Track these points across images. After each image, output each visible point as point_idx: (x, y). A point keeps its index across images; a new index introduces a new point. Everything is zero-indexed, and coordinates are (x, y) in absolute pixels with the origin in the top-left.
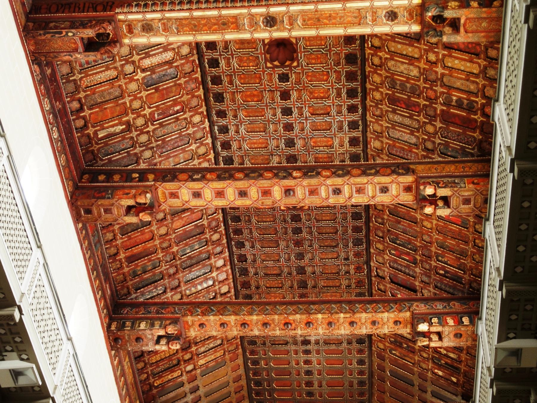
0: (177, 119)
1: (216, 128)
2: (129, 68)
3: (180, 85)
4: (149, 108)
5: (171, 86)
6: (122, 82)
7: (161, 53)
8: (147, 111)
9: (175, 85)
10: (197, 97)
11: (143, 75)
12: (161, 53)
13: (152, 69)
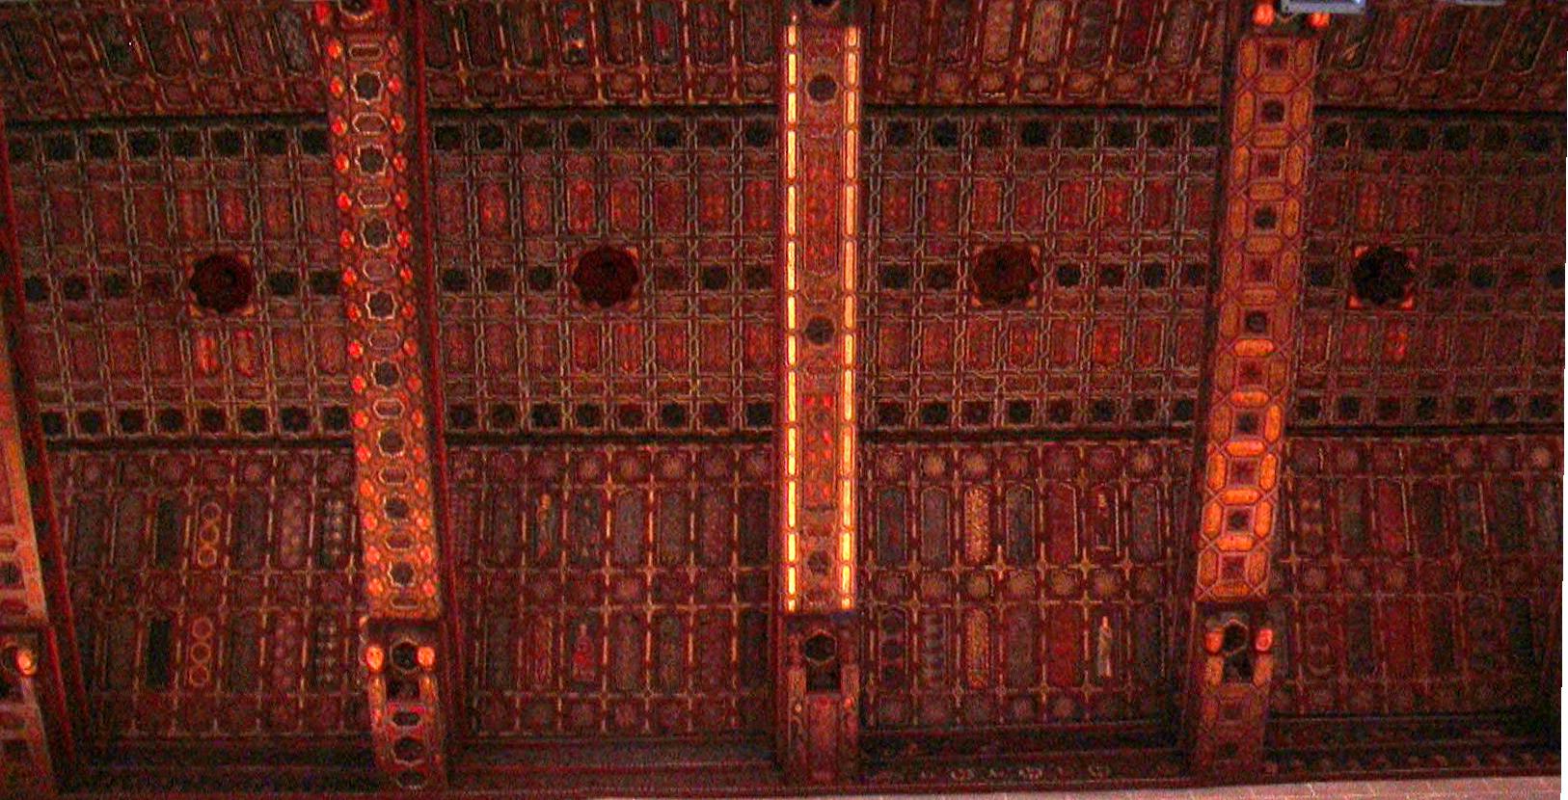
0: (1126, 506)
1: (1176, 424)
3: (1048, 488)
4: (1079, 560)
5: (1046, 509)
6: (1001, 605)
7: (962, 518)
8: (1085, 566)
9: (1045, 497)
10: (1088, 455)
11: (1000, 560)
12: (962, 518)
13: (994, 538)
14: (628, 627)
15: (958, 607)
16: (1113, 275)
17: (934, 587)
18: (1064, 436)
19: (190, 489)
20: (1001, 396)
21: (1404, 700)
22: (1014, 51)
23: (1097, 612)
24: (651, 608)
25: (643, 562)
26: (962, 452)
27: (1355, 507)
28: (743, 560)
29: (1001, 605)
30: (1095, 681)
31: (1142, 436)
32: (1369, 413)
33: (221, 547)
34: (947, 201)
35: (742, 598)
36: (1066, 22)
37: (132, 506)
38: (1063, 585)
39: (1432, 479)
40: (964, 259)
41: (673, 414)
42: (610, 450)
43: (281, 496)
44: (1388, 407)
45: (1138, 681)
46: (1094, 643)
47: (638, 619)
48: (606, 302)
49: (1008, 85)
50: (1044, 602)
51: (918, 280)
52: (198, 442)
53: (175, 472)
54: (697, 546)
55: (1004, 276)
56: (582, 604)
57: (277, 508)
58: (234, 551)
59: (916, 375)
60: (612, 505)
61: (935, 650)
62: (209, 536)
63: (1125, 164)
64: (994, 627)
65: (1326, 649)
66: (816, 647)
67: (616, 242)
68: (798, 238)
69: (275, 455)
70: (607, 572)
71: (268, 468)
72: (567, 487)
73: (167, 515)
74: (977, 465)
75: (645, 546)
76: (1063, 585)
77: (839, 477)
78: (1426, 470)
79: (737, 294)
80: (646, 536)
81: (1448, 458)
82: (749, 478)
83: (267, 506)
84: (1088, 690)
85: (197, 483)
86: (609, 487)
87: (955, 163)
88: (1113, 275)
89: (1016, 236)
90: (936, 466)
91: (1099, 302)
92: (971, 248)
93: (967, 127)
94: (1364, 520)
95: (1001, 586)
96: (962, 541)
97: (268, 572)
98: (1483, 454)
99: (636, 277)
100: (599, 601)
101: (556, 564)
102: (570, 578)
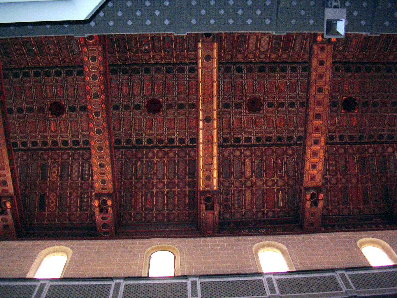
0: (285, 163)
1: (298, 142)
2: (249, 184)
3: (266, 159)
4: (274, 177)
5: (265, 164)
6: (254, 188)
7: (244, 166)
9: (265, 161)
10: (276, 150)
11: (254, 177)
12: (244, 166)
13: (253, 171)
14: (160, 195)
15: (243, 189)
16: (282, 105)
17: (237, 184)
18: (270, 146)
19: (49, 161)
20: (254, 136)
21: (356, 211)
22: (256, 49)
23: (279, 190)
24: (166, 190)
25: (164, 178)
26: (244, 150)
27: (343, 163)
28: (189, 178)
29: (254, 188)
30: (278, 207)
31: (289, 145)
32: (347, 139)
33: (57, 175)
34: (240, 87)
35: (189, 187)
36: (269, 41)
37: (35, 165)
38: (270, 183)
39: (363, 155)
40: (244, 101)
41: (171, 141)
42: (155, 150)
43: (72, 162)
44: (352, 137)
45: (289, 207)
46: (278, 198)
47: (163, 193)
48: (154, 113)
49: (255, 57)
50: (265, 187)
51: (233, 106)
52: (52, 149)
53: (46, 157)
54: (178, 174)
55: (254, 105)
56: (149, 189)
57: (72, 166)
58: (61, 176)
59: (232, 130)
60: (156, 164)
61: (238, 200)
62: (54, 173)
63: (284, 77)
64: (252, 194)
65: (336, 199)
66: (208, 199)
67: (156, 98)
68: (202, 96)
69: (71, 152)
70: (155, 181)
71: (69, 156)
72: (145, 159)
73: (44, 168)
74: (248, 153)
75: (164, 175)
76: (270, 183)
77: (213, 156)
78: (362, 153)
79: (187, 110)
80: (165, 172)
81: (367, 150)
82: (190, 157)
83: (69, 165)
84: (276, 210)
85: (51, 159)
86: (155, 159)
87: (242, 77)
88: (282, 105)
89: (257, 95)
90: (237, 153)
91: (278, 112)
92: (246, 98)
93: (245, 68)
94: (346, 166)
95: (254, 183)
96: (244, 172)
97: (69, 181)
98: (375, 149)
99: (161, 107)
100: (153, 188)
101: (142, 179)
102: (146, 183)
